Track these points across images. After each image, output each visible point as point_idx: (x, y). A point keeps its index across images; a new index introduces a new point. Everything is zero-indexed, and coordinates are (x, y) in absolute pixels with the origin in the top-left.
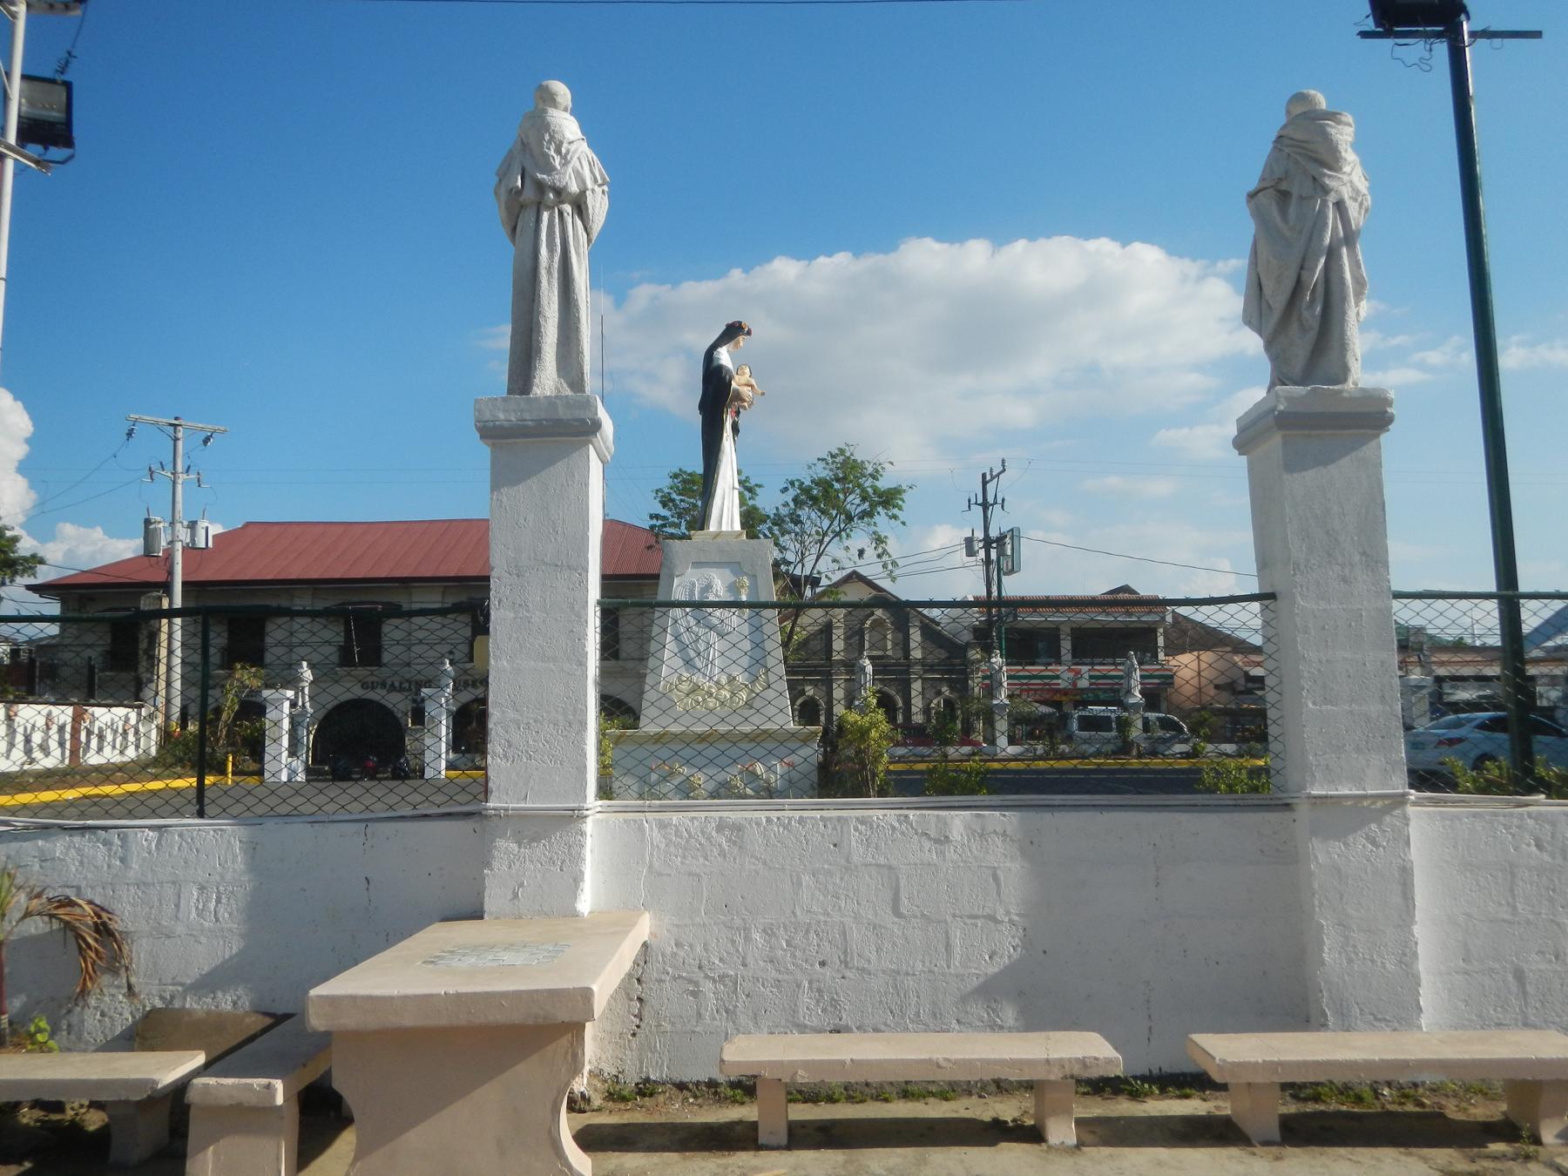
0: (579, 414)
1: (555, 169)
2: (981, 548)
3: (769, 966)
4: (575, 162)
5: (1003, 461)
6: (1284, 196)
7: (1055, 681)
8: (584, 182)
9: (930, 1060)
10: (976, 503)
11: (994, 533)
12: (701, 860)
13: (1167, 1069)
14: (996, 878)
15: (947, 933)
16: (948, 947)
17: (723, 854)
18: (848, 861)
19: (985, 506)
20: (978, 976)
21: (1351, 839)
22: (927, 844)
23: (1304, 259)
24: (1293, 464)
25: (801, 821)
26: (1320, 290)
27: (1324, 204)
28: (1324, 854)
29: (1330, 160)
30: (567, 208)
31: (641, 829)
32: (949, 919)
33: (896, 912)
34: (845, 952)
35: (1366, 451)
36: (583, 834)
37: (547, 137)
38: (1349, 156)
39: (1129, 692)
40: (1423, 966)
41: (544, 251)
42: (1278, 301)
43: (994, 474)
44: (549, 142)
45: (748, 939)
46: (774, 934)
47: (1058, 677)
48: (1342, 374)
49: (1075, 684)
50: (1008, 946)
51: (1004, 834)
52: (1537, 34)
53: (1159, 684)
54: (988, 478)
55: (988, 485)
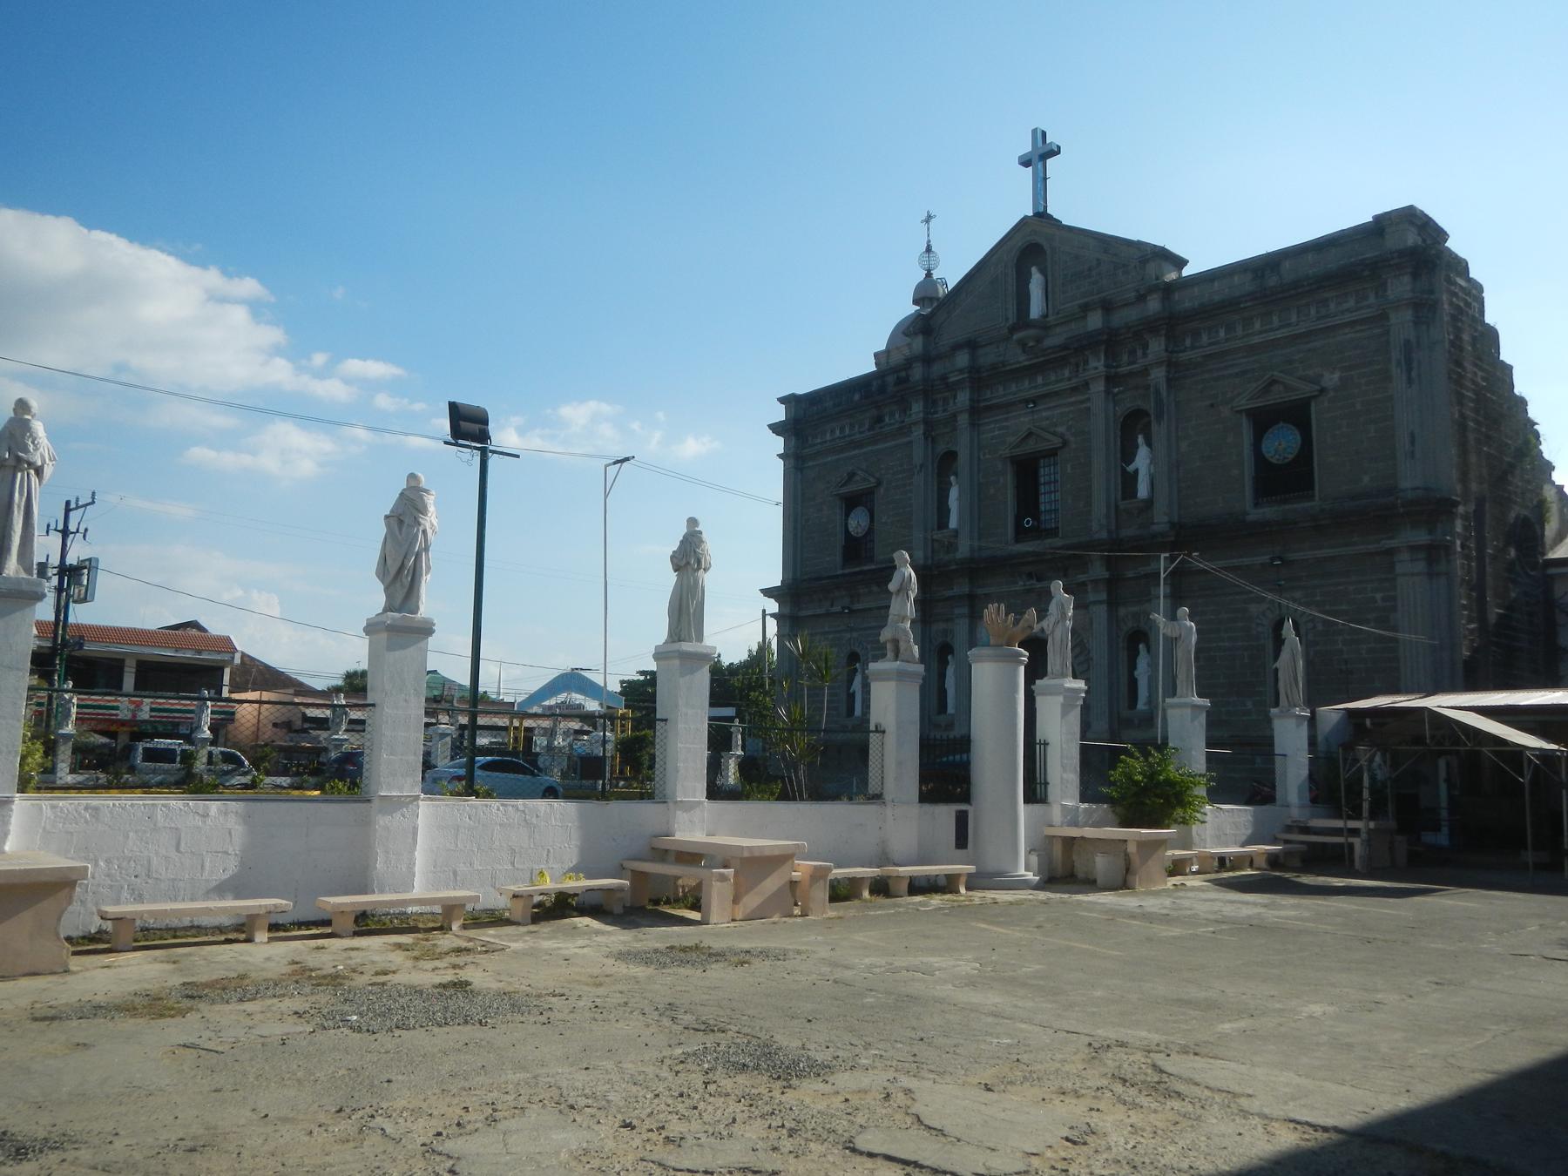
0: (35, 589)
1: (30, 451)
2: (55, 575)
3: (107, 878)
4: (41, 449)
5: (94, 494)
6: (401, 522)
7: (114, 712)
8: (45, 460)
9: (207, 908)
10: (56, 530)
11: (71, 559)
12: (74, 825)
13: (301, 920)
14: (230, 833)
15: (203, 860)
16: (202, 866)
17: (86, 822)
18: (155, 825)
19: (65, 533)
20: (216, 880)
21: (394, 815)
22: (197, 818)
23: (406, 554)
24: (391, 647)
25: (132, 805)
26: (411, 571)
27: (418, 530)
28: (382, 821)
29: (423, 510)
30: (32, 472)
31: (41, 809)
32: (204, 853)
33: (178, 849)
34: (149, 871)
35: (422, 645)
36: (12, 810)
37: (28, 434)
38: (431, 509)
39: (199, 727)
40: (417, 869)
41: (17, 495)
42: (393, 570)
43: (80, 503)
44: (29, 437)
45: (96, 865)
46: (111, 862)
47: (116, 708)
48: (415, 610)
49: (134, 716)
50: (232, 866)
51: (237, 812)
52: (518, 456)
53: (222, 719)
54: (73, 505)
55: (71, 513)
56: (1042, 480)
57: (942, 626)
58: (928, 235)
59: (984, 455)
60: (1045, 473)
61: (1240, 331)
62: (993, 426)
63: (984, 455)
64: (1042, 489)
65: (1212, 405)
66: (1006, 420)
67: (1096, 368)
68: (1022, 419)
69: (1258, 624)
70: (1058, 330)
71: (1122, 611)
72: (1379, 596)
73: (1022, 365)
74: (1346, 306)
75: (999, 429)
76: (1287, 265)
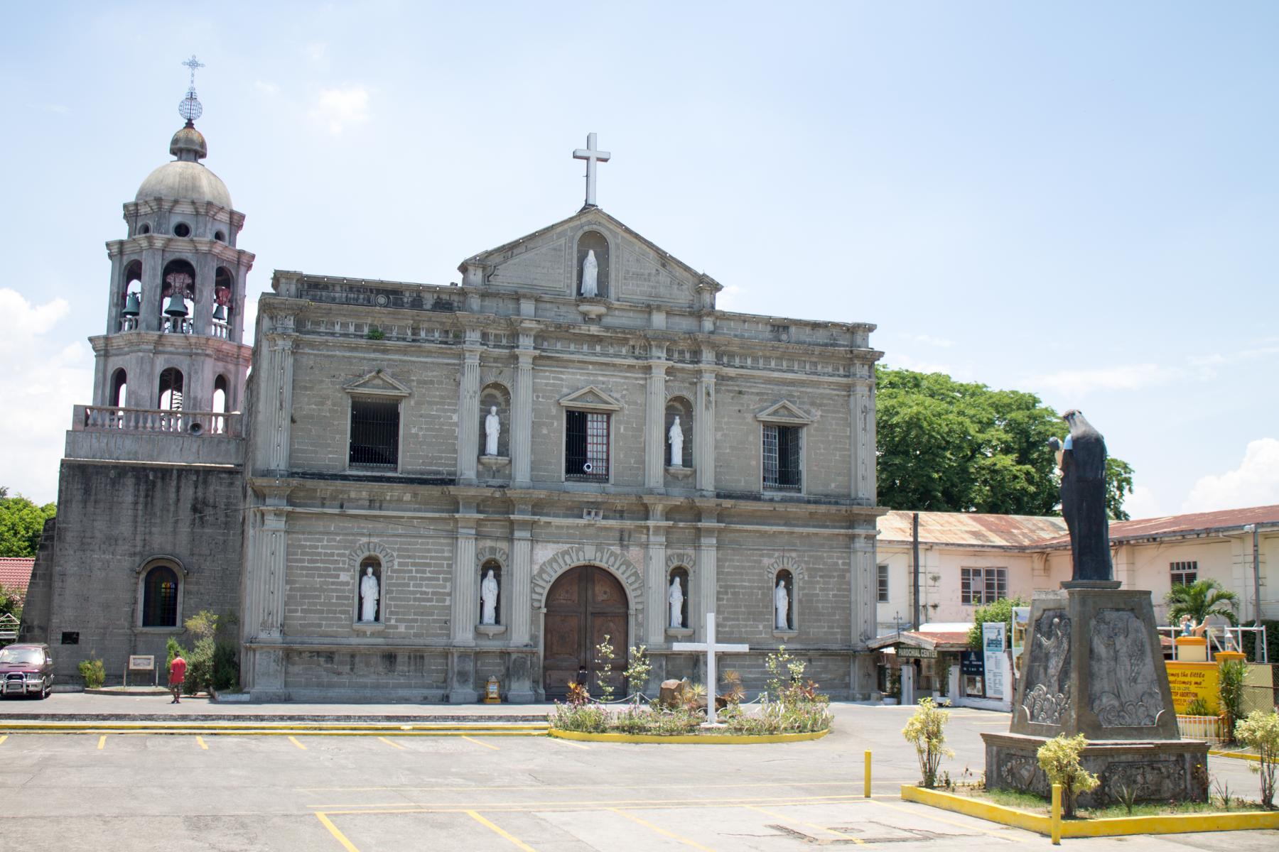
56: (589, 432)
57: (489, 543)
58: (192, 82)
59: (538, 397)
60: (594, 427)
61: (761, 361)
62: (547, 374)
63: (538, 397)
64: (589, 440)
65: (739, 411)
66: (562, 373)
67: (659, 358)
68: (578, 377)
69: (769, 572)
70: (617, 313)
71: (669, 552)
72: (840, 562)
73: (591, 333)
74: (826, 370)
75: (554, 378)
76: (793, 330)
